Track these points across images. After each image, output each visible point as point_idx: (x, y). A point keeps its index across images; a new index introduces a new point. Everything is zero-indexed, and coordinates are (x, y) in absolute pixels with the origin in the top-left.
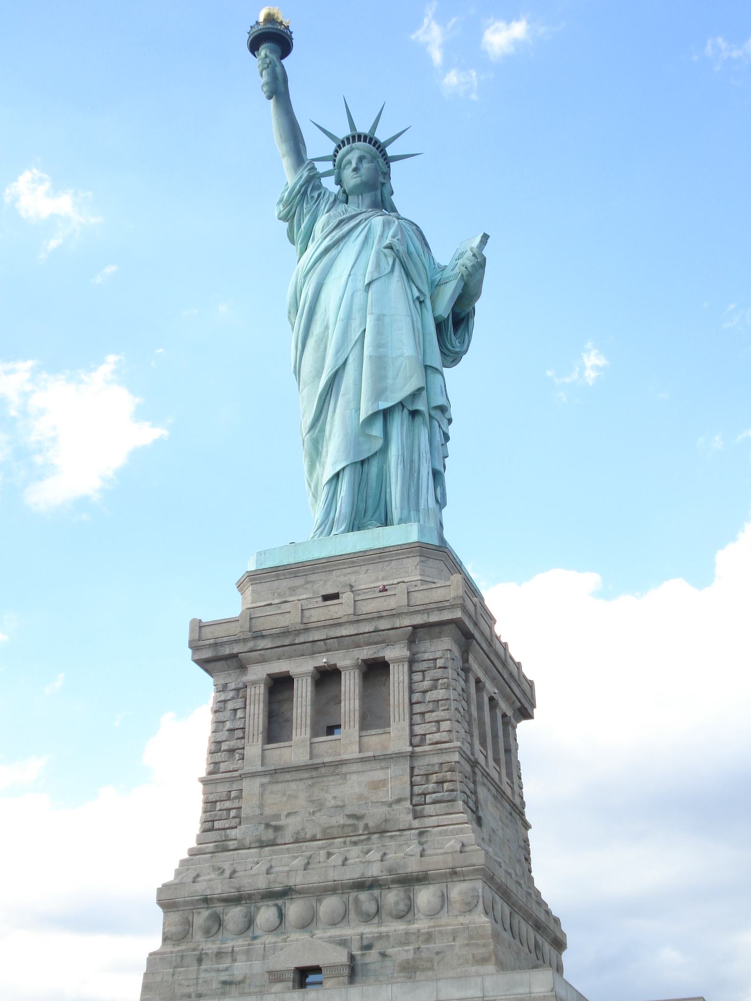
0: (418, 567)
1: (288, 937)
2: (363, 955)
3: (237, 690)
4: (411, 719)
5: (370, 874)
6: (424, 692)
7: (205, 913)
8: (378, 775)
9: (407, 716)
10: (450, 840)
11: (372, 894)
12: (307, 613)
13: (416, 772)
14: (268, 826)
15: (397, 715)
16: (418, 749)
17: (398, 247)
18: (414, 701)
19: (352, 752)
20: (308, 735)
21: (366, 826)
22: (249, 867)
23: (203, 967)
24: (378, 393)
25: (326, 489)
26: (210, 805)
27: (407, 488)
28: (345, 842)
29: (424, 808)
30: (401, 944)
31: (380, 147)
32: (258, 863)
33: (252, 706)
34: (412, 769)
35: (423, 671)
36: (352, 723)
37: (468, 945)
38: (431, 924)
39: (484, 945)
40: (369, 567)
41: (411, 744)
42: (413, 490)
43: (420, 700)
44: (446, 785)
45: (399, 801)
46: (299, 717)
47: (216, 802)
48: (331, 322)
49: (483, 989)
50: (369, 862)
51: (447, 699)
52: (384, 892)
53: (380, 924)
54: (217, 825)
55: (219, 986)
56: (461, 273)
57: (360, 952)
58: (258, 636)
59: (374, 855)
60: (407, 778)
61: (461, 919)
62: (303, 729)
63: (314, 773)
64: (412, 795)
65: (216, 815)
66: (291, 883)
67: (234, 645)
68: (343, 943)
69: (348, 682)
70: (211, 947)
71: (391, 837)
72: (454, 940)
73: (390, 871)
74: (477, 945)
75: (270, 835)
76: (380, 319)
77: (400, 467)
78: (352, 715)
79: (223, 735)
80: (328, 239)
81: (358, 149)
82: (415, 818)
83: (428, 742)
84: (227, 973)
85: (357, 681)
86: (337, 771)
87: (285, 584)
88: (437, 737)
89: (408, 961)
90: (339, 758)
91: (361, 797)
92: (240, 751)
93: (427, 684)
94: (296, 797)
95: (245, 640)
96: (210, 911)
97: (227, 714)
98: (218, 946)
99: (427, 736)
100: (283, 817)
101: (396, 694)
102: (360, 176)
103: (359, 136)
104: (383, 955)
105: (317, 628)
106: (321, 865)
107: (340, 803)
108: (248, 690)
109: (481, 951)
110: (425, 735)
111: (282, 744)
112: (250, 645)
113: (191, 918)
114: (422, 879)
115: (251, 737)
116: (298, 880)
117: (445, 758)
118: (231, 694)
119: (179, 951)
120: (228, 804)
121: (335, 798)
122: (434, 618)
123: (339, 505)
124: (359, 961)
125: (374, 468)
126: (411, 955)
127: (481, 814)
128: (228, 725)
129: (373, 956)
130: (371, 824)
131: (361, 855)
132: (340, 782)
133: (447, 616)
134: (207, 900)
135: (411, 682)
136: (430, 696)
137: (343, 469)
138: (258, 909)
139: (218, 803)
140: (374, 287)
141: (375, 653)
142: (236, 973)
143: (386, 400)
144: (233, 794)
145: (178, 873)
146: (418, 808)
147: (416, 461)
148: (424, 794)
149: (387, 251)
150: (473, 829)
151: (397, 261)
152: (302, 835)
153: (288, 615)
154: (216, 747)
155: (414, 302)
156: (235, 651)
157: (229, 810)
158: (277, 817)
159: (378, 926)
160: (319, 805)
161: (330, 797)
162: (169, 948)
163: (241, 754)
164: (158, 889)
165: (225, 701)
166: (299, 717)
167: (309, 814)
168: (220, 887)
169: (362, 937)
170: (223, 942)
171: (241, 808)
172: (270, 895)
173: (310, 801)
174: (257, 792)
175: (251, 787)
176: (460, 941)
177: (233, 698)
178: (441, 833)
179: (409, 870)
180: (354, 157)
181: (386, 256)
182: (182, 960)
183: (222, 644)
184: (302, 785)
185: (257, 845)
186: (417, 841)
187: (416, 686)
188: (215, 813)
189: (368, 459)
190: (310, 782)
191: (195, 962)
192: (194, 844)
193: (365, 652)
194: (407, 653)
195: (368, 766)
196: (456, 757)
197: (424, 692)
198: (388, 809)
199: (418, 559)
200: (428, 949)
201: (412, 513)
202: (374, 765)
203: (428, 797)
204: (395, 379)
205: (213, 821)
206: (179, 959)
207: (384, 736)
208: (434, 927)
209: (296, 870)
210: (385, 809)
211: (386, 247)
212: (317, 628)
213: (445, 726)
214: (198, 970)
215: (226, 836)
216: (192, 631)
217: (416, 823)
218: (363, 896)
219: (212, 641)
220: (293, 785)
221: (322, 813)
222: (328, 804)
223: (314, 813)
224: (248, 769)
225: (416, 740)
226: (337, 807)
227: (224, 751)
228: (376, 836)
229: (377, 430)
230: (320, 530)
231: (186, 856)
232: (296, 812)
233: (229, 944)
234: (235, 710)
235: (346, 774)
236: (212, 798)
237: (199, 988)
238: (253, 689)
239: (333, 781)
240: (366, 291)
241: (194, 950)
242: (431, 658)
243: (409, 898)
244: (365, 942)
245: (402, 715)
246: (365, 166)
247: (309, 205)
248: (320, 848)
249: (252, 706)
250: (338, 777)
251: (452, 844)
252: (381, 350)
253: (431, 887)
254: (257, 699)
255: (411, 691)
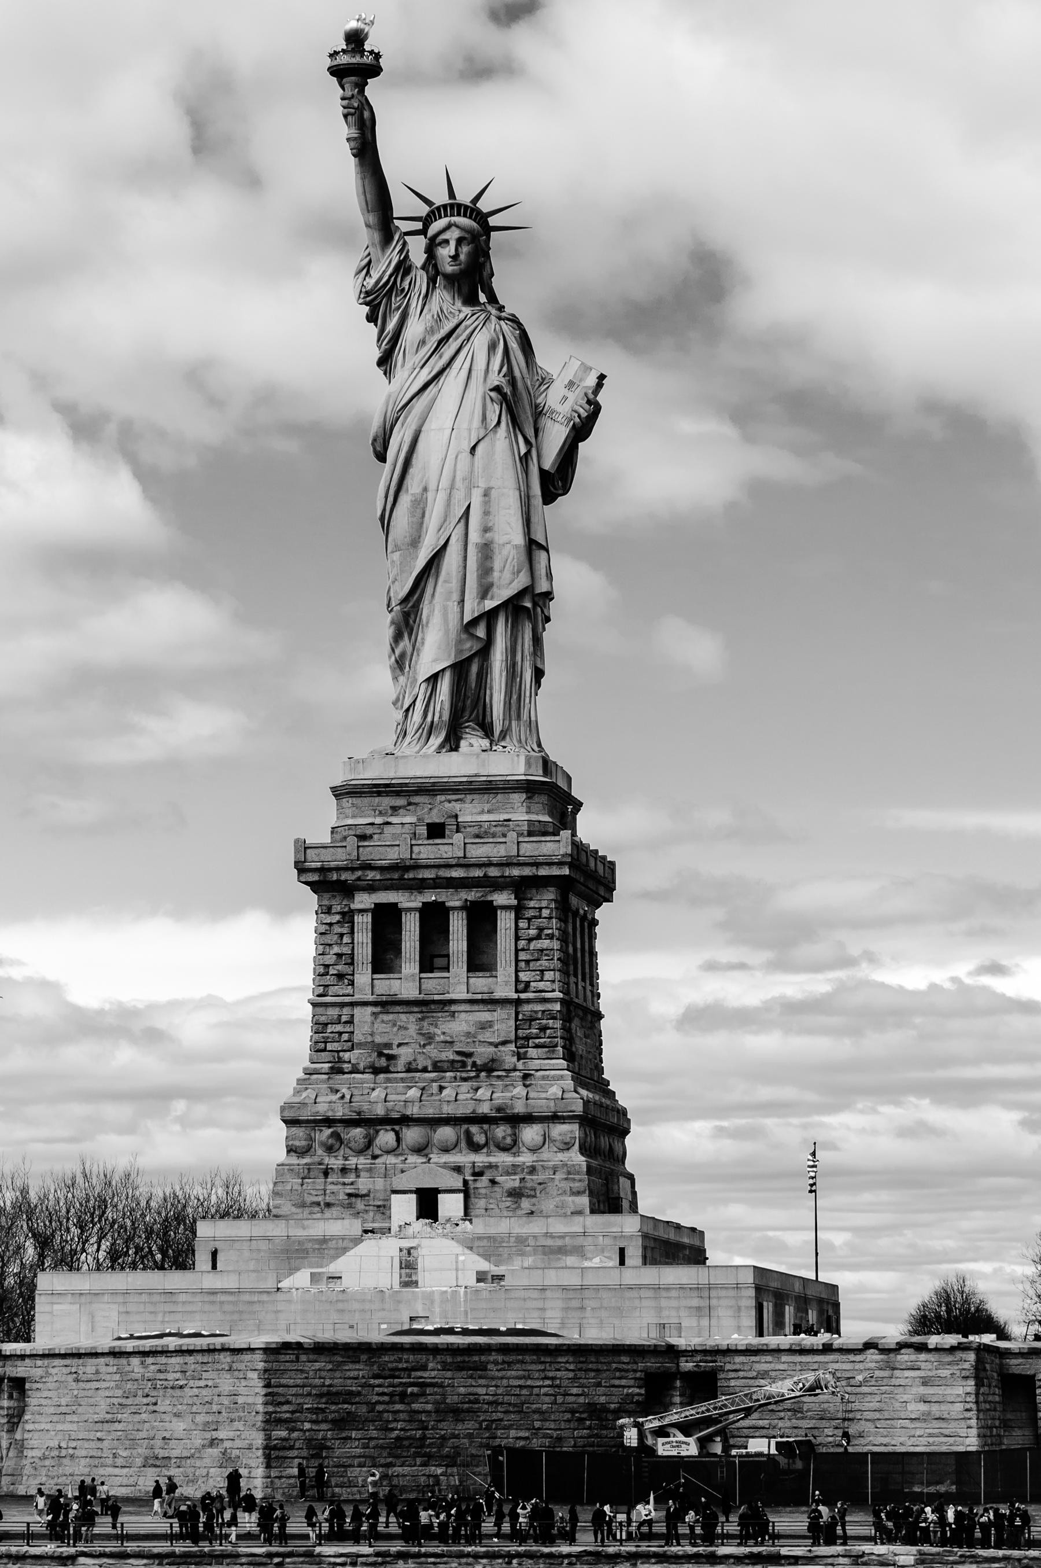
0: (524, 804)
1: (406, 1159)
2: (475, 1180)
3: (343, 914)
4: (516, 965)
5: (480, 1111)
6: (530, 940)
7: (328, 1132)
8: (485, 1016)
9: (513, 964)
10: (552, 1085)
11: (482, 1128)
12: (416, 849)
13: (520, 1017)
14: (380, 1054)
15: (504, 962)
16: (523, 996)
17: (507, 390)
18: (520, 947)
19: (459, 992)
20: (417, 970)
21: (474, 1064)
22: (366, 1092)
23: (329, 1180)
24: (485, 592)
25: (424, 686)
26: (320, 1027)
27: (452, 498)
28: (455, 1078)
29: (527, 1051)
30: (508, 1174)
31: (481, 218)
32: (373, 1089)
33: (360, 934)
34: (517, 1014)
35: (529, 920)
36: (460, 963)
37: (566, 1179)
38: (535, 1159)
39: (580, 1181)
40: (475, 796)
41: (517, 991)
42: (515, 697)
43: (525, 947)
44: (548, 1031)
45: (504, 1043)
46: (408, 951)
47: (328, 1024)
48: (432, 486)
49: (584, 1227)
50: (480, 1100)
51: (551, 950)
52: (493, 1127)
53: (488, 1155)
54: (329, 1047)
55: (346, 1197)
56: (572, 422)
57: (472, 1178)
58: (367, 867)
59: (483, 1093)
60: (512, 1023)
61: (561, 1156)
62: (412, 964)
63: (424, 1009)
64: (517, 1038)
65: (328, 1037)
66: (409, 1113)
67: (342, 872)
68: (458, 1169)
69: (456, 921)
70: (335, 1162)
71: (499, 1077)
72: (554, 1174)
73: (499, 1110)
74: (574, 1179)
75: (383, 1062)
76: (486, 494)
77: (504, 674)
78: (460, 955)
79: (330, 959)
80: (426, 370)
81: (457, 226)
82: (519, 1060)
83: (532, 989)
84: (352, 1187)
85: (465, 922)
86: (446, 1008)
87: (387, 802)
88: (541, 985)
89: (514, 1189)
90: (447, 997)
91: (468, 1034)
92: (350, 977)
93: (533, 932)
94: (406, 1029)
95: (353, 869)
96: (331, 1130)
97: (332, 938)
98: (343, 1162)
99: (532, 983)
100: (395, 1047)
101: (503, 940)
102: (460, 265)
103: (459, 206)
104: (493, 1182)
105: (427, 867)
106: (434, 1098)
107: (448, 1039)
108: (356, 917)
109: (577, 1184)
110: (529, 982)
111: (391, 976)
112: (359, 873)
113: (313, 1135)
114: (529, 1119)
115: (360, 965)
116: (414, 1111)
117: (549, 1006)
118: (337, 918)
119: (306, 1164)
120: (339, 1028)
121: (444, 1033)
122: (543, 872)
123: (438, 709)
124: (471, 1185)
125: (474, 668)
126: (517, 1184)
127: (574, 1049)
128: (336, 949)
129: (484, 1181)
130: (479, 1062)
131: (471, 1091)
132: (449, 1019)
133: (555, 871)
134: (328, 1122)
135: (517, 928)
136: (535, 945)
137: (443, 670)
138: (377, 1132)
139: (330, 1026)
140: (479, 449)
141: (482, 896)
142: (361, 1187)
143: (492, 598)
144: (344, 1018)
145: (297, 1092)
146: (522, 1050)
147: (520, 664)
148: (527, 1038)
149: (493, 394)
150: (572, 1076)
151: (504, 405)
152: (414, 1066)
153: (397, 848)
154: (323, 971)
155: (521, 459)
156: (343, 878)
157: (340, 1033)
158: (388, 1046)
159: (488, 1156)
160: (430, 1038)
161: (439, 1032)
162: (294, 1160)
163: (349, 980)
164: (281, 1107)
165: (331, 924)
166: (408, 951)
167: (420, 1046)
168: (340, 1112)
169: (474, 1166)
170: (346, 1159)
171: (353, 1033)
172: (386, 1121)
173: (421, 1034)
174: (369, 1020)
175: (364, 1015)
176: (559, 1176)
177: (338, 922)
178: (544, 1078)
179: (516, 1111)
180: (453, 235)
181: (492, 400)
182: (309, 1172)
183: (330, 870)
184: (412, 1018)
185: (371, 1070)
186: (521, 1083)
187: (521, 933)
188: (326, 1035)
189: (469, 660)
190: (419, 1016)
191: (322, 1175)
192: (307, 1064)
193: (473, 893)
194: (515, 902)
195: (476, 1007)
196: (557, 1007)
197: (530, 940)
198: (494, 1049)
199: (524, 796)
200: (532, 1180)
201: (513, 723)
202: (481, 1007)
203: (531, 1041)
204: (501, 571)
205: (325, 1042)
206: (306, 1171)
207: (490, 979)
208: (537, 1161)
209: (413, 1102)
210: (492, 1049)
211: (491, 390)
212: (427, 867)
213: (549, 975)
214: (325, 1182)
215: (339, 1057)
216: (297, 851)
217: (520, 1065)
218: (474, 1129)
219: (319, 864)
220: (403, 1017)
221: (432, 1046)
222: (437, 1039)
223: (424, 1046)
224: (358, 997)
225: (521, 986)
226: (446, 1042)
227: (332, 975)
228: (483, 1074)
229: (481, 632)
230: (418, 734)
231: (301, 1075)
232: (407, 1043)
233: (353, 1161)
234: (341, 935)
235: (454, 1012)
236: (323, 1019)
237: (327, 1198)
238: (360, 916)
239: (442, 1017)
240: (471, 453)
241: (320, 1164)
242: (537, 906)
243: (515, 1135)
244: (477, 1170)
245: (508, 962)
246: (465, 249)
247: (398, 299)
248: (433, 1081)
249: (360, 934)
250: (448, 1014)
251: (555, 1091)
252: (488, 535)
253: (534, 1126)
254: (365, 927)
255: (517, 938)
